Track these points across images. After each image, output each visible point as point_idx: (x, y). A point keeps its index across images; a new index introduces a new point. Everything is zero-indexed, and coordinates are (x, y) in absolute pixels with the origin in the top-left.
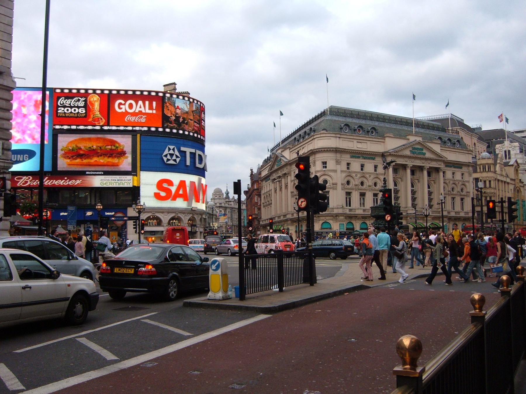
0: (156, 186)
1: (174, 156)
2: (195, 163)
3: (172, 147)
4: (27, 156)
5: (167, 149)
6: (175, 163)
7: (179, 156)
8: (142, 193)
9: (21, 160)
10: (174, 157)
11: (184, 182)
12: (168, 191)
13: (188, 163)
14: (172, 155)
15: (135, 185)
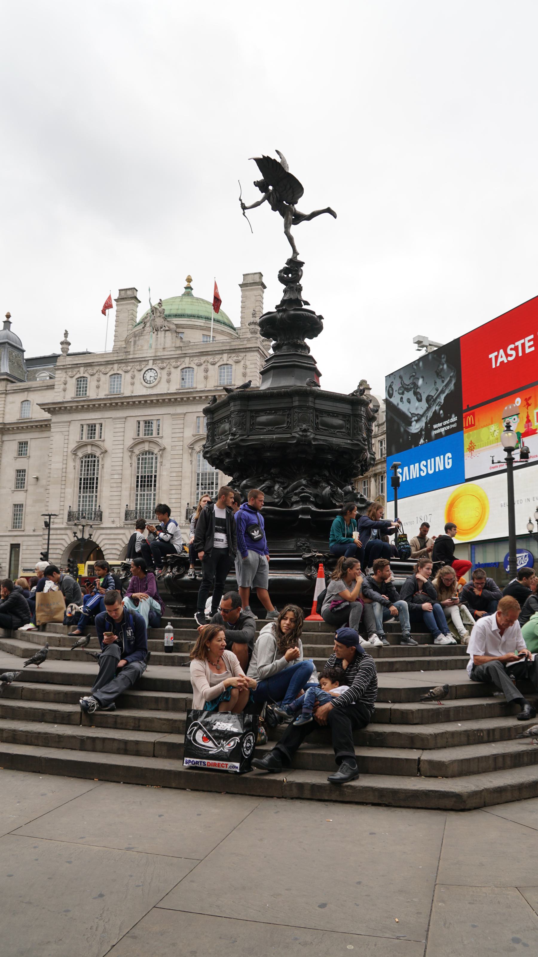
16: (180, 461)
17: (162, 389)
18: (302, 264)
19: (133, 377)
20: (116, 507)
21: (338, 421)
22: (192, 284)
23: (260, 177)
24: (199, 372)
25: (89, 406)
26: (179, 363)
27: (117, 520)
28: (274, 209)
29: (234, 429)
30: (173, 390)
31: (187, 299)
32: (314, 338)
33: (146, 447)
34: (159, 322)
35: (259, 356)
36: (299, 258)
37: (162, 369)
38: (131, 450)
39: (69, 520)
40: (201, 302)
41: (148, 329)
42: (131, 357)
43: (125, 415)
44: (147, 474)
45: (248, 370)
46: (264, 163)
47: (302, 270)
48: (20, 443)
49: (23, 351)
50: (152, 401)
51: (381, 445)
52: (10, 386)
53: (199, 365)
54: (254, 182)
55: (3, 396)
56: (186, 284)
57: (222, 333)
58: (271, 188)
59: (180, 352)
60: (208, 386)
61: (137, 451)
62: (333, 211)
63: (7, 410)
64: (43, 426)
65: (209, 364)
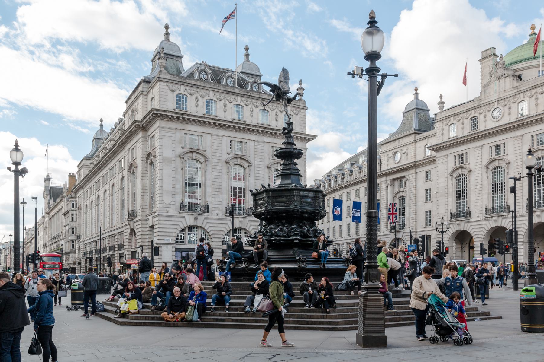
17: (506, 120)
19: (485, 117)
20: (480, 206)
25: (457, 142)
26: (516, 99)
27: (480, 215)
30: (513, 120)
33: (497, 163)
34: (500, 72)
37: (505, 106)
38: (487, 167)
39: (451, 218)
41: (493, 79)
42: (482, 102)
43: (482, 144)
44: (498, 182)
48: (426, 172)
49: (428, 110)
50: (497, 131)
52: (418, 137)
55: (414, 144)
59: (516, 91)
61: (491, 167)
63: (417, 153)
64: (433, 161)
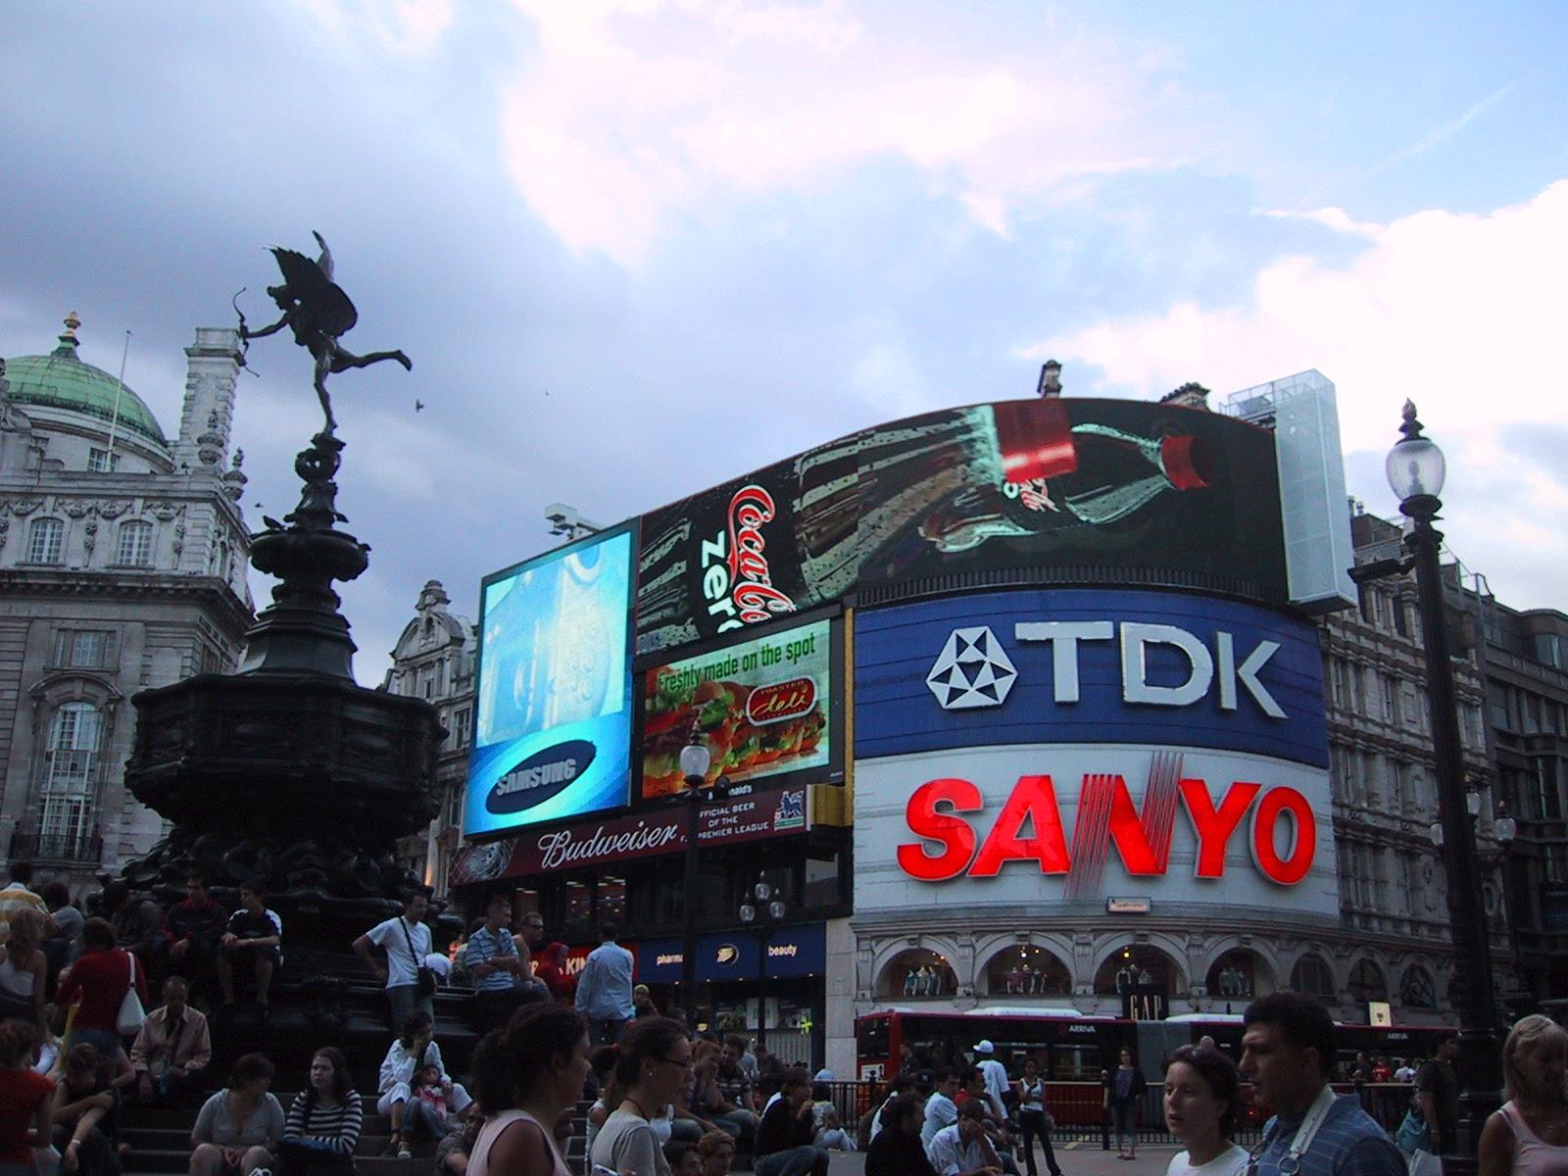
0: (904, 817)
1: (986, 670)
2: (1121, 688)
3: (971, 635)
4: (572, 762)
5: (952, 642)
6: (990, 702)
7: (1009, 667)
8: (860, 856)
9: (559, 779)
10: (985, 676)
11: (1045, 781)
12: (948, 832)
13: (1066, 686)
14: (971, 670)
15: (822, 821)
16: (9, 724)
18: (341, 445)
21: (380, 743)
22: (77, 333)
23: (280, 281)
24: (75, 535)
26: (30, 507)
28: (300, 342)
29: (192, 744)
31: (64, 366)
32: (350, 581)
35: (214, 511)
36: (337, 434)
40: (95, 376)
45: (187, 539)
46: (288, 260)
47: (339, 456)
51: (461, 722)
53: (76, 516)
54: (269, 289)
56: (64, 331)
57: (137, 450)
58: (298, 302)
60: (91, 566)
62: (406, 358)
65: (98, 517)
